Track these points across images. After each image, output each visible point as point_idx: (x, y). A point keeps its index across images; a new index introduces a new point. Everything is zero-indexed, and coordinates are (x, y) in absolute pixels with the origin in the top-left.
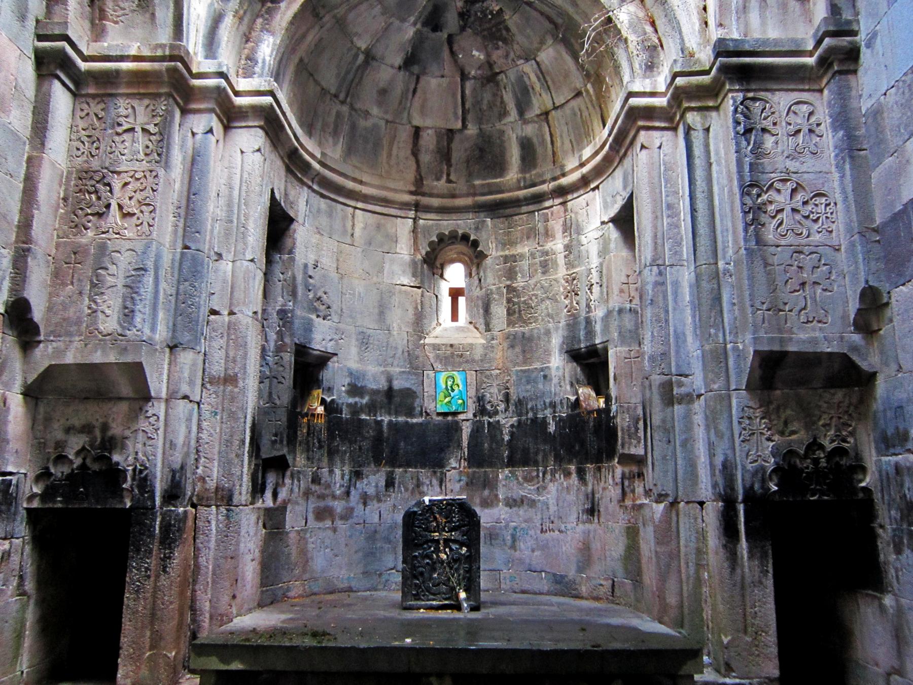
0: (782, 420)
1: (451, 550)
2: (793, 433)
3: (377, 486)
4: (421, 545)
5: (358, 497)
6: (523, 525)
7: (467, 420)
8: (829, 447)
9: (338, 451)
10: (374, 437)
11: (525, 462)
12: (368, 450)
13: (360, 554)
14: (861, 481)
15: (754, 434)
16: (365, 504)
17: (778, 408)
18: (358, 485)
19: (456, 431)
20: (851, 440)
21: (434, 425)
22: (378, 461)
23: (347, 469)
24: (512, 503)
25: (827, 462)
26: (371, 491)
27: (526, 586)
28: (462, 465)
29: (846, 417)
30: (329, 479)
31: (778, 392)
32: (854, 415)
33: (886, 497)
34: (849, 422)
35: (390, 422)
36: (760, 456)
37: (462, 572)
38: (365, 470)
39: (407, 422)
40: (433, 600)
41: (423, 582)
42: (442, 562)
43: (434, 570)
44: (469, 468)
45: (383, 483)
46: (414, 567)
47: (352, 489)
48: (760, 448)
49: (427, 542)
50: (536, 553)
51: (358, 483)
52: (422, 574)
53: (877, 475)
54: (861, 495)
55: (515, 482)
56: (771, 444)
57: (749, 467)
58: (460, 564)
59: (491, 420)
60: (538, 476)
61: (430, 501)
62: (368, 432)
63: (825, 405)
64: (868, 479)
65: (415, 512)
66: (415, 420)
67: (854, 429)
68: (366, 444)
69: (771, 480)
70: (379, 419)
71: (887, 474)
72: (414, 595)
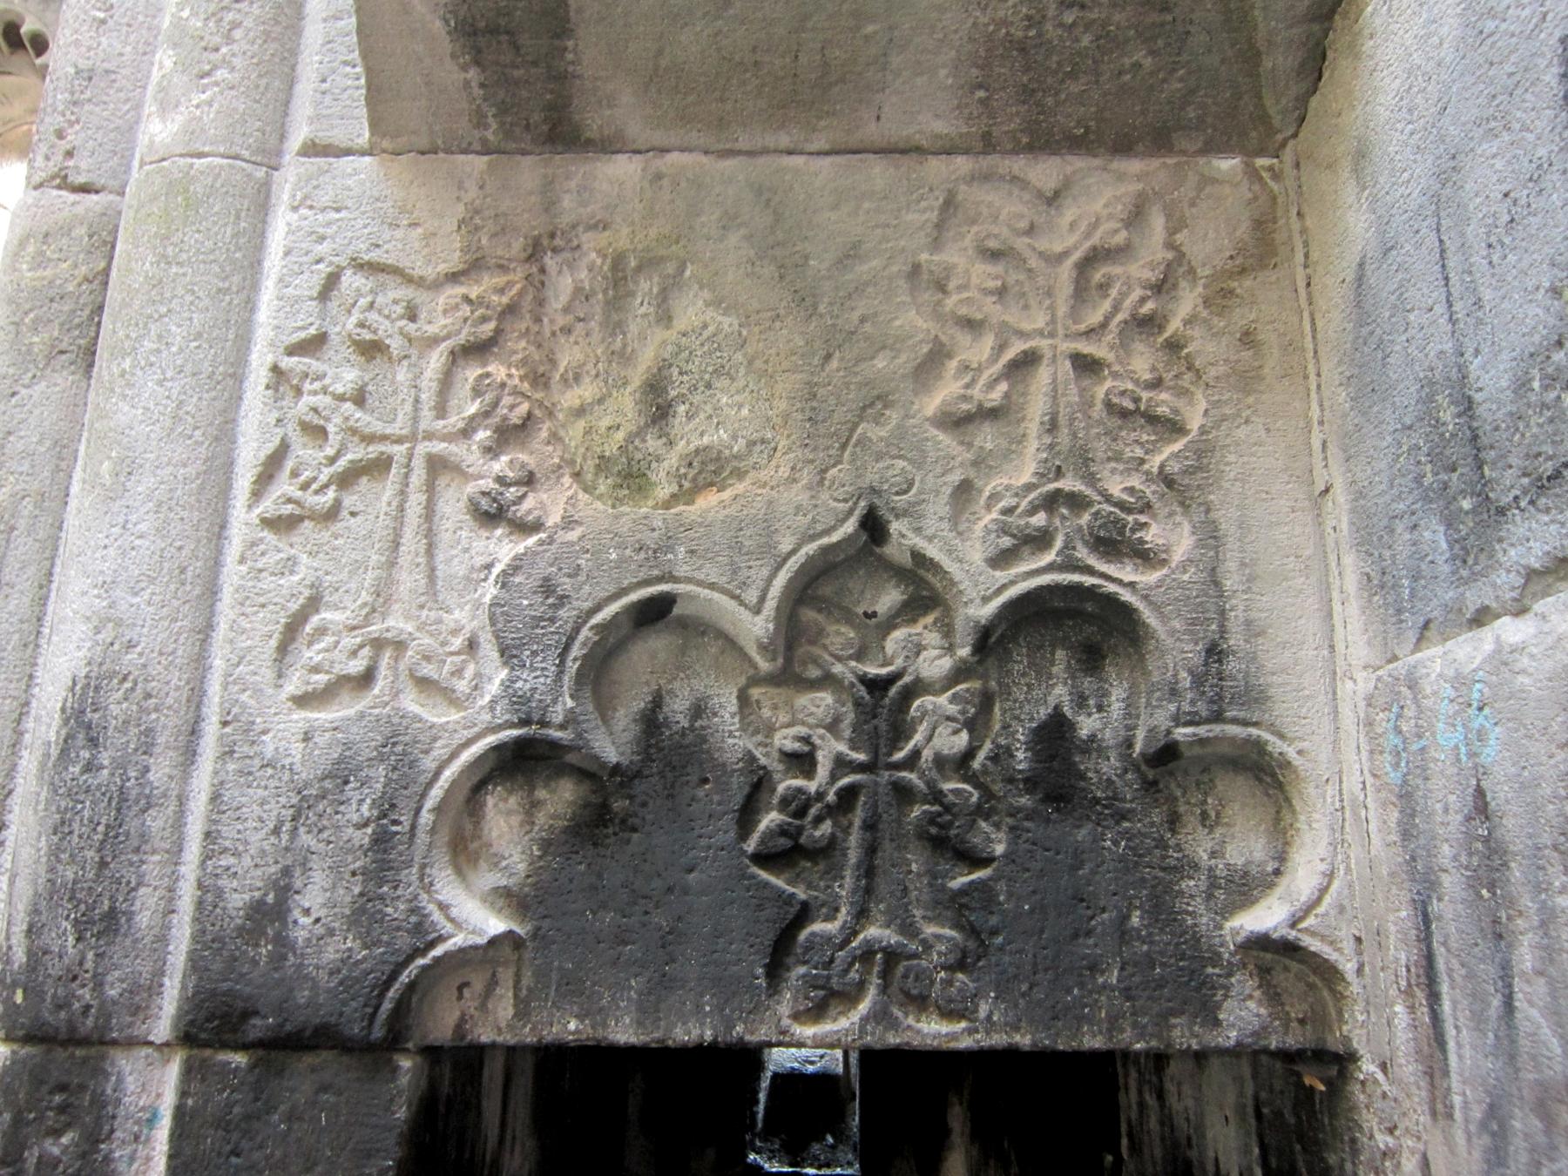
0: (637, 376)
2: (709, 470)
8: (982, 588)
14: (1246, 888)
15: (378, 467)
17: (619, 277)
20: (1173, 536)
25: (975, 724)
29: (1143, 362)
31: (624, 168)
32: (1205, 347)
33: (1466, 1053)
34: (1164, 403)
36: (400, 646)
48: (409, 580)
53: (1381, 823)
54: (1243, 1014)
56: (504, 548)
57: (293, 735)
63: (983, 273)
64: (1303, 877)
67: (1203, 451)
69: (464, 848)
71: (1481, 806)
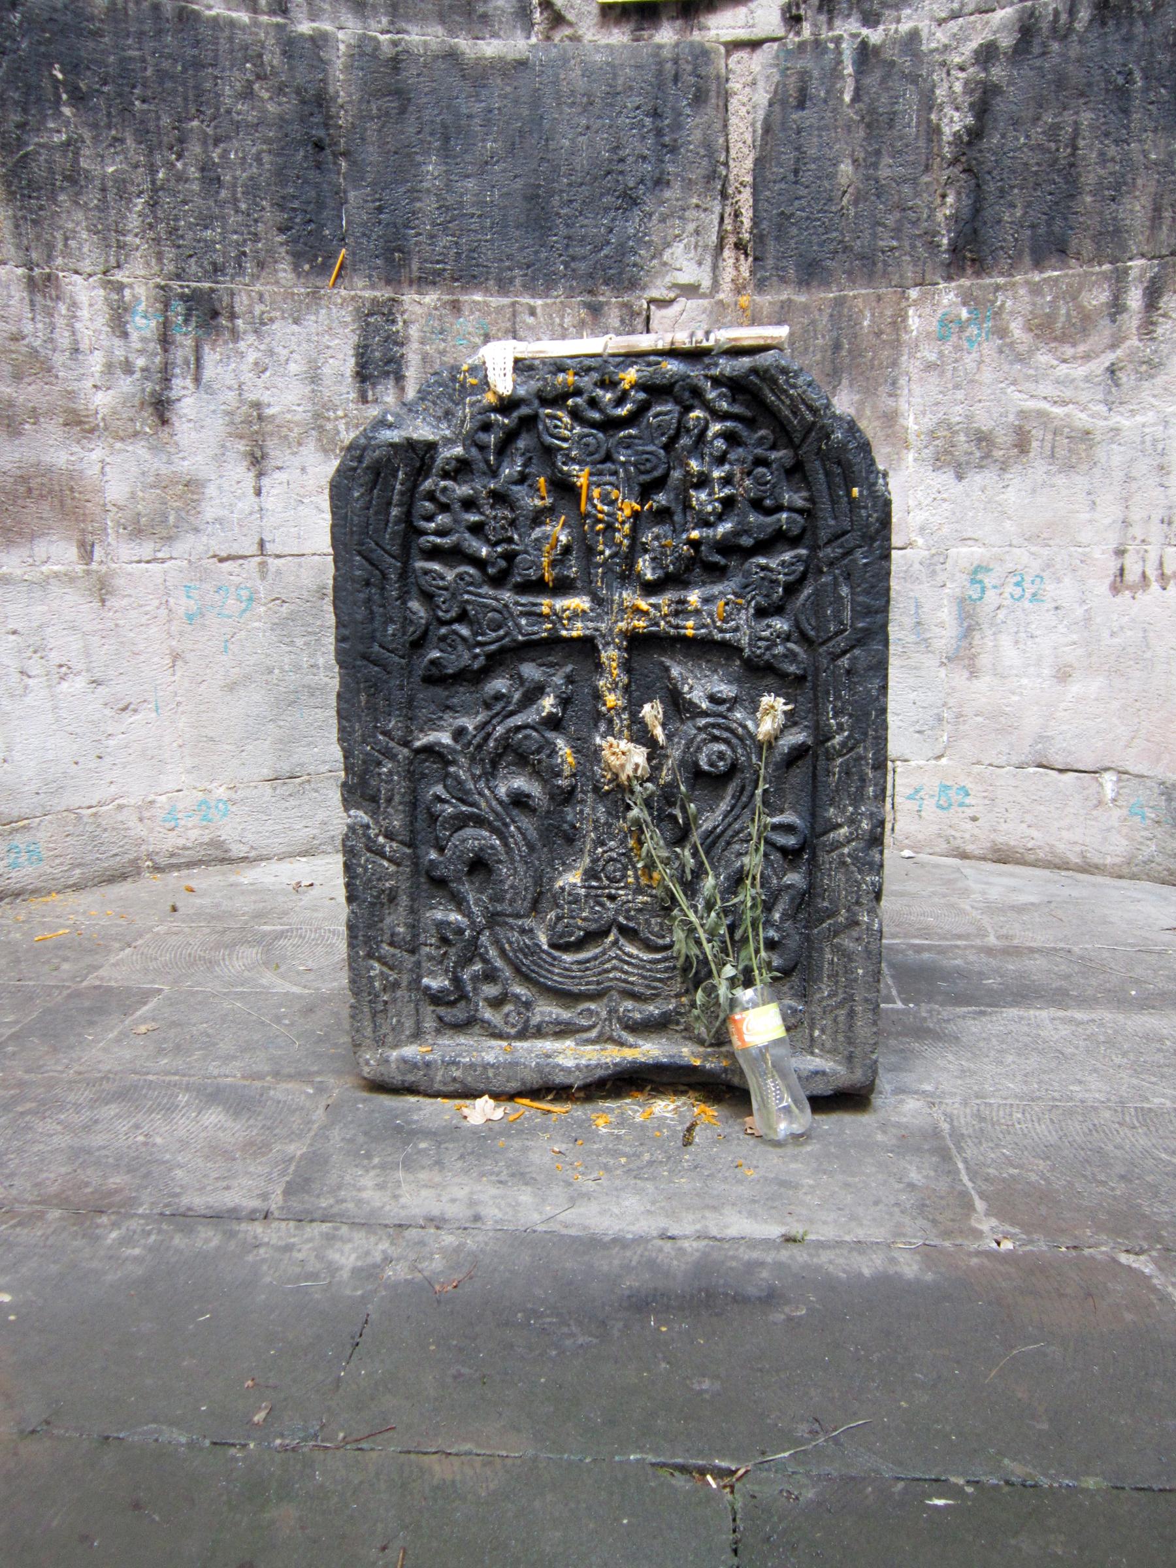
1: (678, 706)
3: (314, 377)
4: (474, 677)
5: (217, 426)
6: (1021, 556)
7: (754, 45)
9: (75, 178)
10: (282, 120)
11: (1050, 247)
12: (253, 189)
13: (254, 698)
16: (257, 461)
18: (209, 372)
19: (699, 99)
21: (588, 72)
22: (314, 252)
23: (140, 280)
24: (971, 451)
26: (286, 399)
27: (1013, 833)
28: (728, 274)
30: (34, 330)
35: (364, 51)
37: (753, 862)
38: (245, 294)
39: (452, 56)
40: (564, 1030)
41: (494, 919)
42: (617, 795)
43: (561, 838)
44: (761, 285)
45: (341, 362)
46: (423, 825)
47: (181, 384)
49: (504, 657)
50: (1075, 689)
51: (211, 357)
52: (479, 865)
55: (989, 348)
58: (743, 803)
59: (875, 36)
60: (1117, 307)
61: (521, 366)
62: (247, 94)
65: (419, 456)
66: (490, 48)
68: (245, 159)
70: (305, 28)
72: (436, 999)
